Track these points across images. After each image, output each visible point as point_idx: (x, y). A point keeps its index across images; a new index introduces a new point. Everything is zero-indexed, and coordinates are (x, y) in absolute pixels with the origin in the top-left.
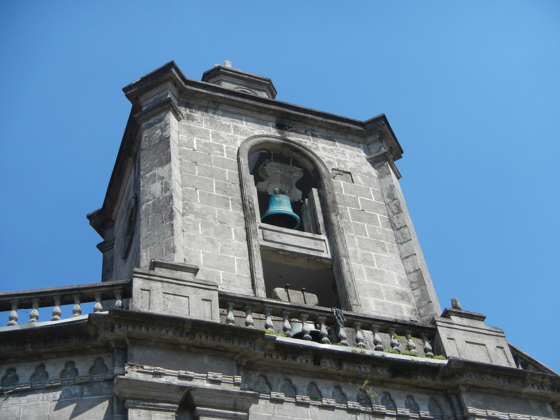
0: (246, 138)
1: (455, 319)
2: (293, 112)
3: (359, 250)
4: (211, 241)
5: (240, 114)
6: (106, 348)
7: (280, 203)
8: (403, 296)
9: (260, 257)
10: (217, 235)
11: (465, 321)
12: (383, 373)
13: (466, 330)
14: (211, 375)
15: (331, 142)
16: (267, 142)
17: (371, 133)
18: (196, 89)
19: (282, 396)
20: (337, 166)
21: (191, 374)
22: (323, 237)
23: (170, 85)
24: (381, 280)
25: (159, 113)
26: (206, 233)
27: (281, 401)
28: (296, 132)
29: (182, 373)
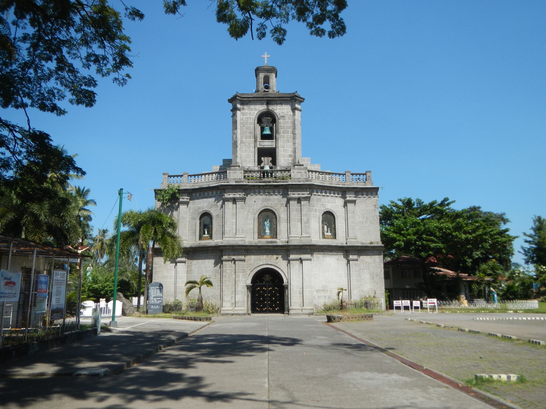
0: (257, 112)
1: (296, 167)
2: (271, 99)
3: (282, 144)
4: (246, 150)
5: (257, 102)
6: (222, 189)
7: (266, 130)
8: (290, 156)
9: (257, 153)
10: (248, 148)
11: (298, 167)
12: (272, 187)
13: (298, 169)
14: (239, 193)
15: (281, 105)
16: (263, 112)
17: (293, 99)
18: (244, 99)
19: (253, 194)
20: (281, 115)
21: (235, 194)
22: (274, 141)
23: (237, 101)
24: (286, 152)
25: (235, 111)
26: (245, 148)
27: (253, 195)
28: (272, 104)
29: (234, 194)
